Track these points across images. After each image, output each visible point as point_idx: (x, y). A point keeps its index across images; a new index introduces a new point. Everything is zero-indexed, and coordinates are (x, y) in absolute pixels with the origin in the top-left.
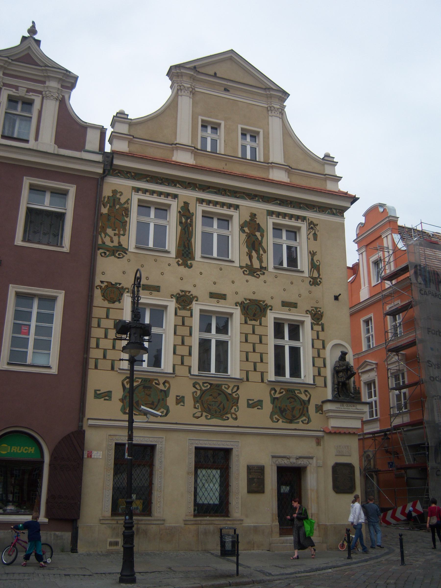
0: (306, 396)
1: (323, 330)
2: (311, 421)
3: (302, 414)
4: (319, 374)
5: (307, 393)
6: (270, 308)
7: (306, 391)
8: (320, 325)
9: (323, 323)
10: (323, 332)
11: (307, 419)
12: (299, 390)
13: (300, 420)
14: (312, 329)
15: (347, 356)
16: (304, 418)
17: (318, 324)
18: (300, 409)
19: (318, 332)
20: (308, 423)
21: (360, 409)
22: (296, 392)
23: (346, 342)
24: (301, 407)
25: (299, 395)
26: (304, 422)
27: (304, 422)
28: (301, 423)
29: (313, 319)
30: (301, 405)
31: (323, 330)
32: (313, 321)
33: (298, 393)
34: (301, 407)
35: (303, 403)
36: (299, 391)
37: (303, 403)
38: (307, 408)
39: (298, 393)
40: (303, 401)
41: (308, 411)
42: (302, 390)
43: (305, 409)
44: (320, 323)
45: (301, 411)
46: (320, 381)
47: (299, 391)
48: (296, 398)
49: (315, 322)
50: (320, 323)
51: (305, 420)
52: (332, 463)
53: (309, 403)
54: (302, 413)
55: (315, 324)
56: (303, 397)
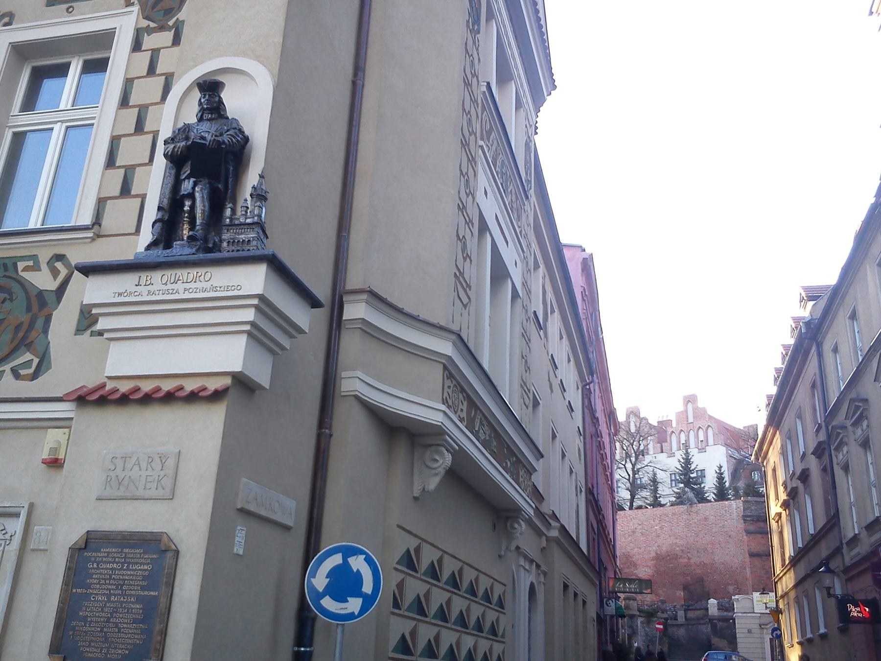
0: (55, 273)
1: (176, 41)
2: (49, 367)
3: (22, 343)
4: (126, 190)
5: (59, 265)
6: (6, 20)
7: (60, 258)
8: (169, 29)
9: (181, 19)
10: (176, 49)
11: (36, 361)
12: (34, 258)
13: (7, 368)
14: (137, 46)
15: (233, 100)
16: (28, 356)
17: (162, 28)
18: (18, 327)
19: (155, 53)
20: (34, 376)
21: (228, 288)
22: (21, 265)
23: (258, 58)
24: (25, 318)
25: (28, 276)
26: (23, 372)
27: (23, 372)
28: (8, 376)
29: (147, 18)
30: (29, 309)
31: (176, 41)
32: (145, 23)
33: (25, 269)
34: (25, 318)
35: (34, 301)
36: (31, 263)
37: (34, 301)
38: (48, 319)
39: (25, 269)
40: (41, 294)
41: (46, 330)
42: (44, 256)
43: (40, 322)
44: (171, 23)
45: (21, 335)
46: (120, 214)
47: (31, 263)
48: (16, 288)
49: (152, 25)
50: (171, 23)
51: (28, 364)
52: (73, 534)
53: (59, 300)
54: (24, 338)
55: (149, 31)
56: (43, 281)
